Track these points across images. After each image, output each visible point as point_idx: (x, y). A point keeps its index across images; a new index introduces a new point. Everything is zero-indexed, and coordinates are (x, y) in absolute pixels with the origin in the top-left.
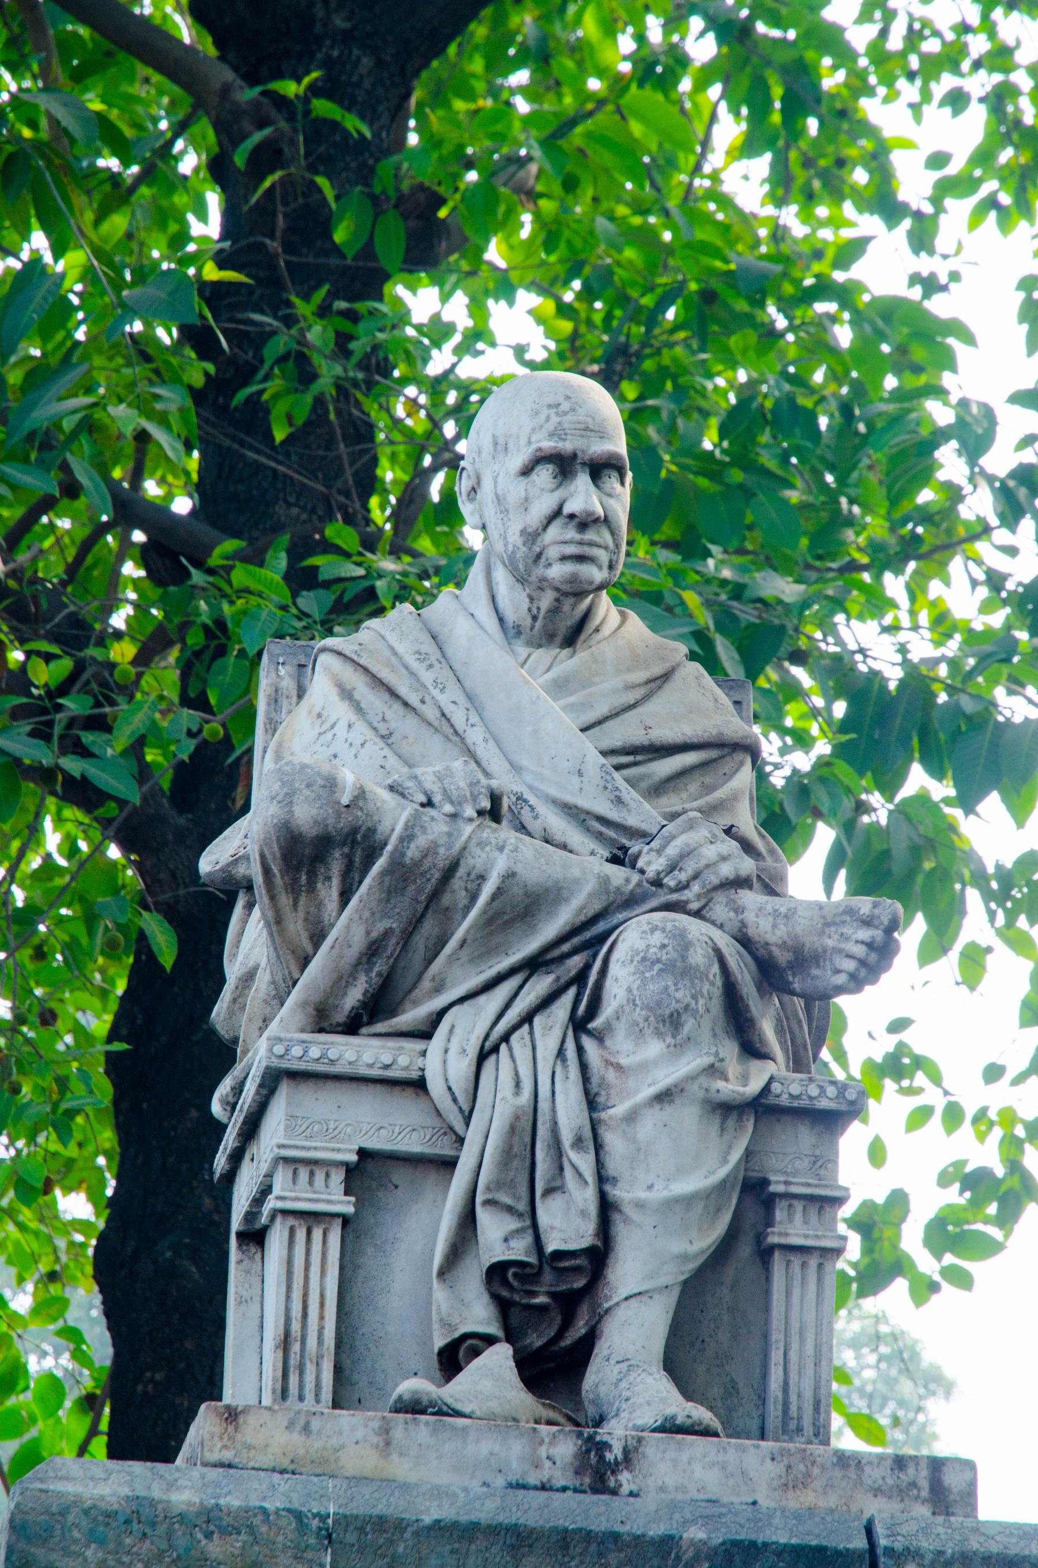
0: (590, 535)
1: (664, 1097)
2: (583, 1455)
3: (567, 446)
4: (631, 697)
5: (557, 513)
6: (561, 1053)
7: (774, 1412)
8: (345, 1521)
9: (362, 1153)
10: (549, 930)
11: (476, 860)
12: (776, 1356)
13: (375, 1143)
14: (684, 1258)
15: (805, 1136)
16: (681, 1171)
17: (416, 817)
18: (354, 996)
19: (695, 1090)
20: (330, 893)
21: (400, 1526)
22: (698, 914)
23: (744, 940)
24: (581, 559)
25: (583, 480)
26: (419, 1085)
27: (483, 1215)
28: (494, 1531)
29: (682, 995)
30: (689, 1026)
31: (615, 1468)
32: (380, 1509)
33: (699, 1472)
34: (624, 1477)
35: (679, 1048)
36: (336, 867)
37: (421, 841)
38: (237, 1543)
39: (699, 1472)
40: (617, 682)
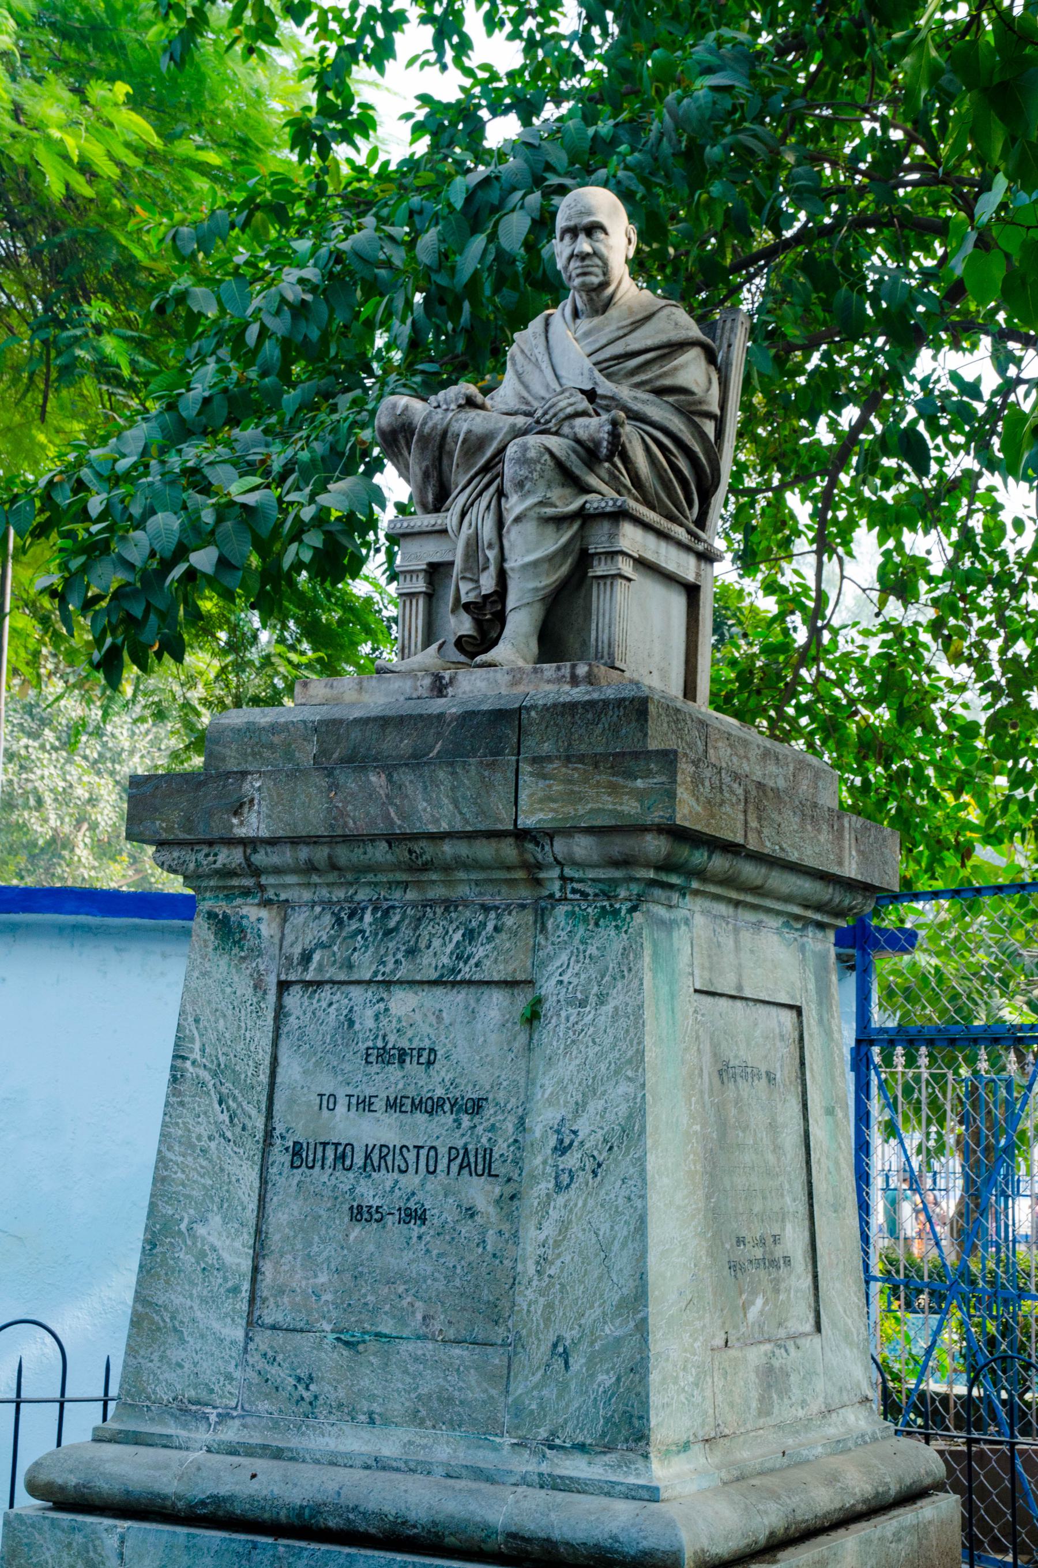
0: (587, 262)
1: (518, 519)
2: (434, 683)
3: (572, 223)
4: (621, 333)
5: (571, 256)
6: (488, 507)
7: (592, 650)
8: (320, 722)
9: (431, 565)
10: (489, 453)
11: (455, 427)
12: (594, 626)
13: (435, 559)
14: (536, 590)
15: (606, 526)
16: (528, 552)
17: (430, 413)
18: (430, 497)
19: (532, 514)
20: (405, 453)
21: (341, 722)
22: (556, 433)
23: (578, 441)
24: (584, 274)
25: (582, 237)
26: (444, 531)
27: (461, 584)
28: (375, 719)
29: (524, 472)
30: (528, 485)
31: (446, 686)
32: (337, 716)
33: (479, 684)
34: (450, 690)
35: (524, 497)
36: (402, 442)
37: (430, 424)
38: (283, 736)
39: (479, 684)
40: (614, 327)
